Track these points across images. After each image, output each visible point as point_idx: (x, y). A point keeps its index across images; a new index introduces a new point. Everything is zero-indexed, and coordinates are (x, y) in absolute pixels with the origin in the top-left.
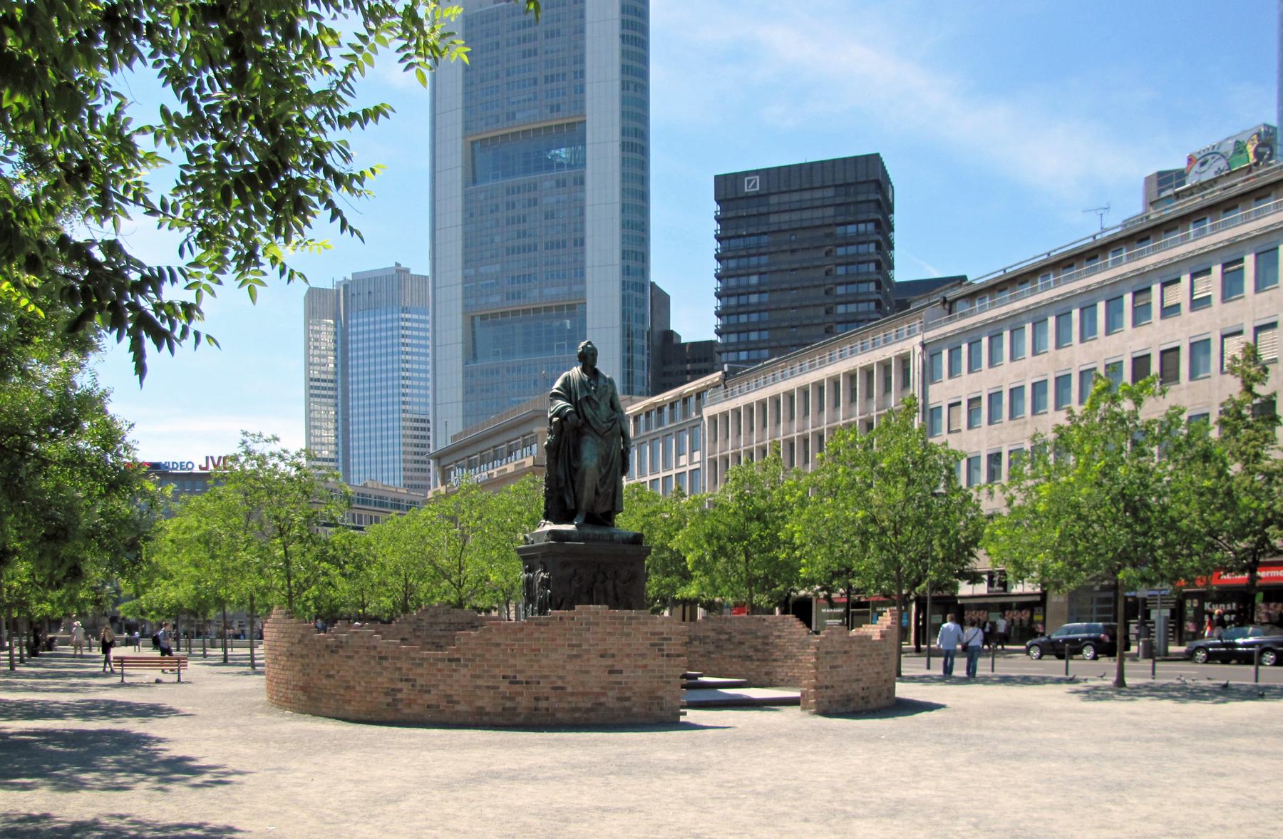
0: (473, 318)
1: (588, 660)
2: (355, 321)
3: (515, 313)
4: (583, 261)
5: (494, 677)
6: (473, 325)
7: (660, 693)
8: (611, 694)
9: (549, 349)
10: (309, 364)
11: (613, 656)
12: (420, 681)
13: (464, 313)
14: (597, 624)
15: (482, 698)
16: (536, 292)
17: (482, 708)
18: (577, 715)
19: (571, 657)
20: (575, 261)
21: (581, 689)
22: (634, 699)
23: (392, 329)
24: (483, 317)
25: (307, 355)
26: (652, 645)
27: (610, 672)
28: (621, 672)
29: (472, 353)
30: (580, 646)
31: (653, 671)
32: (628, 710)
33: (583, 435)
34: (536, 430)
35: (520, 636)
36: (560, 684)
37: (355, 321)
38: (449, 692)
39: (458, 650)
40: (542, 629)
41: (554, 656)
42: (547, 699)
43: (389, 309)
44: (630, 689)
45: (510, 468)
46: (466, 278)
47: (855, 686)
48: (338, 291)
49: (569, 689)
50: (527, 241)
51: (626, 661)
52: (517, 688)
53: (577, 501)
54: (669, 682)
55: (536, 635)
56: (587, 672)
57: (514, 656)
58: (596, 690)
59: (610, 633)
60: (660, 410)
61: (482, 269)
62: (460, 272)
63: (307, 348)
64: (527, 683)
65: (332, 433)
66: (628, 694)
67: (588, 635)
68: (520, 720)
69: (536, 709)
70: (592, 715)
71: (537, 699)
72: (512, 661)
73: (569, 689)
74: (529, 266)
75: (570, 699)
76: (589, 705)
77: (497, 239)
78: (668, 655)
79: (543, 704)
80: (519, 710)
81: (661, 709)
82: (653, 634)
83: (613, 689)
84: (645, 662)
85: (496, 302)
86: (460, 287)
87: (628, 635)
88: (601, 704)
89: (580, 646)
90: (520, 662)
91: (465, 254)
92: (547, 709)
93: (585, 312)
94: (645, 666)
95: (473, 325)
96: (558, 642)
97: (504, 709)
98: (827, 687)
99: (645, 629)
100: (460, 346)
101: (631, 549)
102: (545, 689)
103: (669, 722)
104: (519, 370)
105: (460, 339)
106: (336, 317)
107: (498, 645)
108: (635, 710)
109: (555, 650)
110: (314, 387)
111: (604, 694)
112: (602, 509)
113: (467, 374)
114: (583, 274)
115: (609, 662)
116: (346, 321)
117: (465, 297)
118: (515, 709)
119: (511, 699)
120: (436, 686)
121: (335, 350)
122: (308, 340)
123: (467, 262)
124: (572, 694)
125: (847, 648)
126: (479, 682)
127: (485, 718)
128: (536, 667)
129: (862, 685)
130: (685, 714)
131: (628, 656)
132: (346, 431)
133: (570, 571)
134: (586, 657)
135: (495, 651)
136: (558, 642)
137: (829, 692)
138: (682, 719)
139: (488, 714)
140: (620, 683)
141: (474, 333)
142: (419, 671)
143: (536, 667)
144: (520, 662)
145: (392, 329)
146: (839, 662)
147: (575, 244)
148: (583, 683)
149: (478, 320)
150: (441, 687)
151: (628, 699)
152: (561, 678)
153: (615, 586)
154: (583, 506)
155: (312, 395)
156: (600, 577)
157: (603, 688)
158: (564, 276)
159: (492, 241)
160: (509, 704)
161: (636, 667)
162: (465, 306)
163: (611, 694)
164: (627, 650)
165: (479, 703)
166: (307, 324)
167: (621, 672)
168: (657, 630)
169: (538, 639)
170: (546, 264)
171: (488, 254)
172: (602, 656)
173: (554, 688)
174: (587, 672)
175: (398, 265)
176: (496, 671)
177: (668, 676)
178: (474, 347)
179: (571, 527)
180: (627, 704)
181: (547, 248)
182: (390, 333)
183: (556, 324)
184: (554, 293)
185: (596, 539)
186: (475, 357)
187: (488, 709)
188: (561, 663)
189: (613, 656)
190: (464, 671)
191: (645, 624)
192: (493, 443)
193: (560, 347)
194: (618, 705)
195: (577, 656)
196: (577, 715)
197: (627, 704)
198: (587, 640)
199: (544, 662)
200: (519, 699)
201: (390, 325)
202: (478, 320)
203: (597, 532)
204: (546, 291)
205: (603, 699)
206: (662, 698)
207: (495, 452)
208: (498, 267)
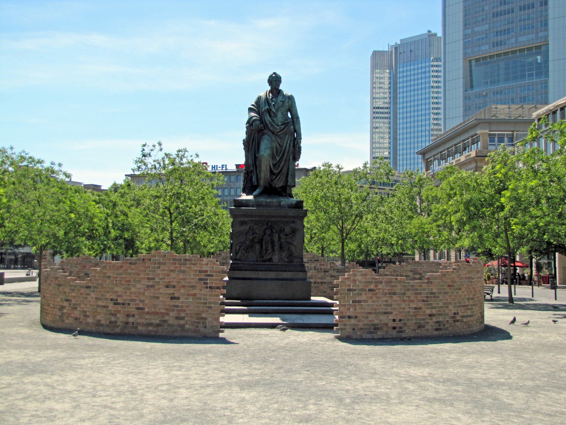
0: (470, 61)
1: (159, 289)
2: (401, 70)
3: (498, 55)
4: (547, 16)
5: (106, 299)
6: (471, 66)
7: (204, 315)
8: (172, 314)
9: (523, 77)
10: (373, 98)
11: (174, 287)
12: (73, 302)
13: (464, 59)
14: (165, 264)
15: (100, 313)
16: (513, 40)
17: (100, 321)
18: (150, 328)
19: (149, 287)
20: (541, 16)
21: (153, 310)
22: (186, 318)
23: (425, 73)
24: (477, 60)
25: (372, 93)
26: (200, 279)
27: (172, 298)
28: (179, 298)
29: (470, 84)
30: (154, 279)
31: (200, 298)
32: (182, 326)
33: (264, 134)
34: (479, 132)
35: (121, 271)
36: (141, 305)
37: (401, 70)
38: (85, 309)
39: (90, 280)
40: (133, 266)
41: (138, 286)
42: (133, 316)
43: (424, 60)
44: (184, 311)
45: (463, 158)
46: (465, 36)
47: (383, 318)
48: (391, 52)
49: (146, 310)
50: (507, 7)
51: (182, 291)
52: (119, 307)
53: (258, 180)
54: (211, 307)
55: (129, 271)
56: (158, 298)
57: (117, 285)
58: (162, 311)
59: (172, 270)
60: (554, 113)
61: (476, 29)
62: (461, 32)
63: (373, 88)
64: (123, 304)
65: (387, 141)
66: (183, 315)
67: (159, 271)
68: (118, 330)
69: (127, 323)
70: (160, 329)
71: (128, 316)
72: (116, 289)
73: (146, 310)
74: (508, 24)
75: (147, 317)
76: (158, 322)
77: (486, 8)
78: (210, 288)
79: (131, 320)
80: (118, 323)
81: (205, 327)
82: (201, 271)
83: (173, 310)
84: (194, 292)
85: (485, 49)
86: (461, 42)
87: (184, 272)
88: (165, 321)
89: (154, 279)
90: (119, 289)
91: (465, 20)
92: (133, 323)
93: (547, 51)
94: (195, 295)
95: (471, 66)
96: (142, 276)
97: (111, 322)
98: (349, 317)
99: (195, 268)
100: (461, 81)
101: (292, 212)
102: (132, 309)
103: (210, 335)
104: (501, 93)
105: (461, 76)
106: (390, 68)
107: (109, 277)
108: (187, 326)
109: (139, 282)
110: (375, 111)
111: (167, 314)
112: (279, 184)
113: (466, 98)
114: (546, 24)
115: (171, 291)
116: (396, 70)
117: (465, 48)
118: (116, 322)
119: (114, 315)
120: (80, 305)
121: (390, 88)
122: (373, 83)
123: (466, 26)
124: (148, 313)
125: (372, 287)
126: (100, 303)
127: (101, 328)
128: (128, 294)
129: (391, 317)
130: (222, 332)
131: (184, 286)
132: (395, 139)
133: (246, 228)
134: (157, 287)
135: (108, 281)
136: (142, 276)
137: (353, 321)
138: (221, 335)
139: (102, 325)
140: (177, 306)
141: (471, 71)
142: (74, 294)
143: (128, 294)
144: (119, 289)
145: (425, 73)
146: (364, 297)
147: (541, 5)
148: (155, 306)
149: (473, 63)
150: (82, 306)
151: (183, 318)
152: (142, 301)
153: (280, 238)
154: (262, 183)
155: (374, 118)
156: (268, 232)
157: (167, 309)
158: (533, 27)
159: (483, 10)
160: (113, 319)
161: (188, 295)
162: (465, 54)
163: (172, 314)
164: (183, 283)
165: (98, 317)
166: (372, 73)
167: (179, 298)
168: (204, 269)
169: (130, 274)
170: (520, 21)
171: (480, 18)
172: (167, 287)
173: (138, 309)
174: (158, 298)
175: (429, 31)
176: (108, 296)
177: (210, 303)
178: (471, 80)
179: (250, 197)
180: (182, 322)
181: (520, 10)
182: (424, 75)
183: (531, 59)
184: (526, 39)
185: (267, 205)
186: (472, 87)
187: (102, 322)
188: (142, 290)
189: (174, 287)
190: (93, 295)
191: (195, 264)
192: (455, 142)
193: (531, 75)
194: (176, 322)
195: (152, 286)
196: (150, 328)
197: (182, 322)
198: (158, 275)
199: (133, 290)
200: (118, 315)
201: (423, 70)
202: (473, 63)
203: (268, 200)
204: (521, 39)
205: (167, 318)
206: (206, 319)
207: (456, 148)
208: (487, 27)
